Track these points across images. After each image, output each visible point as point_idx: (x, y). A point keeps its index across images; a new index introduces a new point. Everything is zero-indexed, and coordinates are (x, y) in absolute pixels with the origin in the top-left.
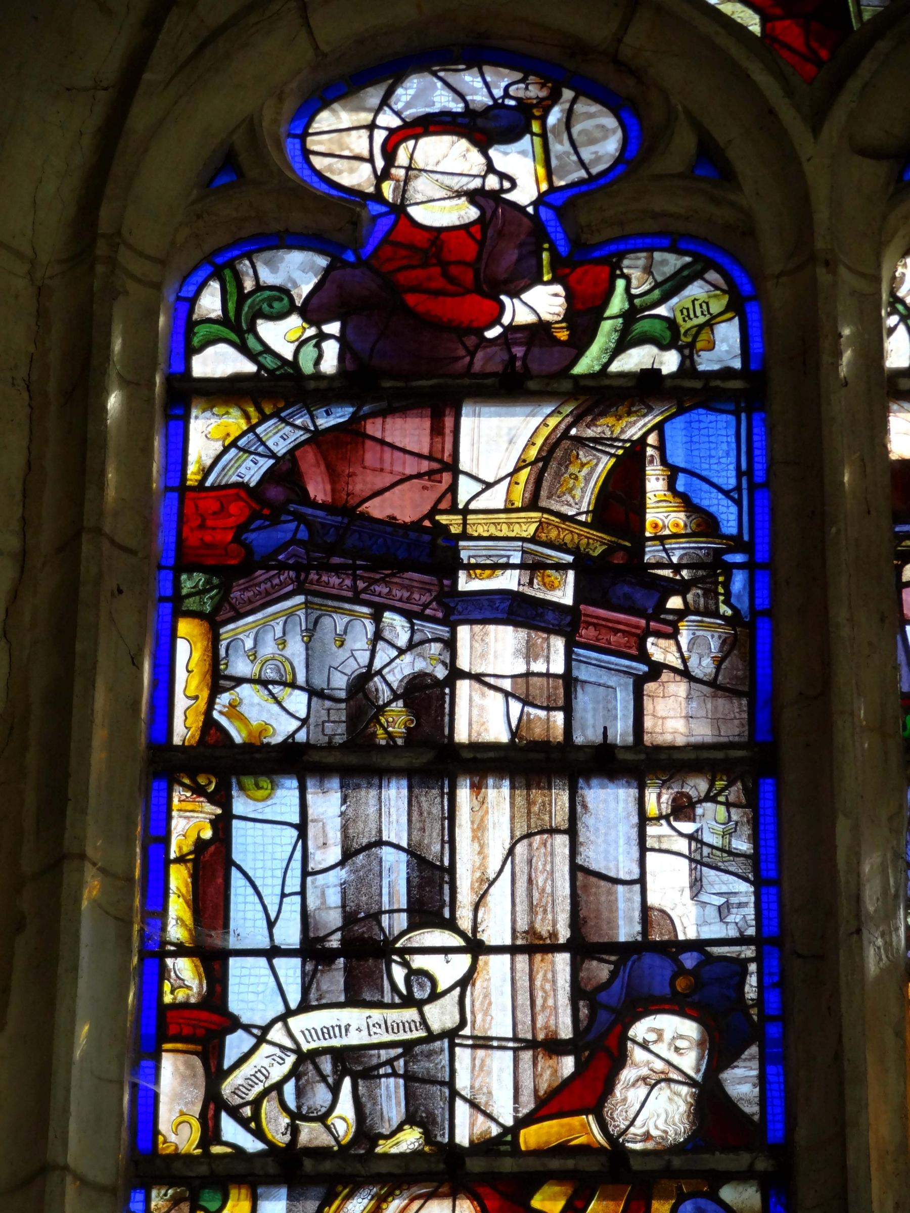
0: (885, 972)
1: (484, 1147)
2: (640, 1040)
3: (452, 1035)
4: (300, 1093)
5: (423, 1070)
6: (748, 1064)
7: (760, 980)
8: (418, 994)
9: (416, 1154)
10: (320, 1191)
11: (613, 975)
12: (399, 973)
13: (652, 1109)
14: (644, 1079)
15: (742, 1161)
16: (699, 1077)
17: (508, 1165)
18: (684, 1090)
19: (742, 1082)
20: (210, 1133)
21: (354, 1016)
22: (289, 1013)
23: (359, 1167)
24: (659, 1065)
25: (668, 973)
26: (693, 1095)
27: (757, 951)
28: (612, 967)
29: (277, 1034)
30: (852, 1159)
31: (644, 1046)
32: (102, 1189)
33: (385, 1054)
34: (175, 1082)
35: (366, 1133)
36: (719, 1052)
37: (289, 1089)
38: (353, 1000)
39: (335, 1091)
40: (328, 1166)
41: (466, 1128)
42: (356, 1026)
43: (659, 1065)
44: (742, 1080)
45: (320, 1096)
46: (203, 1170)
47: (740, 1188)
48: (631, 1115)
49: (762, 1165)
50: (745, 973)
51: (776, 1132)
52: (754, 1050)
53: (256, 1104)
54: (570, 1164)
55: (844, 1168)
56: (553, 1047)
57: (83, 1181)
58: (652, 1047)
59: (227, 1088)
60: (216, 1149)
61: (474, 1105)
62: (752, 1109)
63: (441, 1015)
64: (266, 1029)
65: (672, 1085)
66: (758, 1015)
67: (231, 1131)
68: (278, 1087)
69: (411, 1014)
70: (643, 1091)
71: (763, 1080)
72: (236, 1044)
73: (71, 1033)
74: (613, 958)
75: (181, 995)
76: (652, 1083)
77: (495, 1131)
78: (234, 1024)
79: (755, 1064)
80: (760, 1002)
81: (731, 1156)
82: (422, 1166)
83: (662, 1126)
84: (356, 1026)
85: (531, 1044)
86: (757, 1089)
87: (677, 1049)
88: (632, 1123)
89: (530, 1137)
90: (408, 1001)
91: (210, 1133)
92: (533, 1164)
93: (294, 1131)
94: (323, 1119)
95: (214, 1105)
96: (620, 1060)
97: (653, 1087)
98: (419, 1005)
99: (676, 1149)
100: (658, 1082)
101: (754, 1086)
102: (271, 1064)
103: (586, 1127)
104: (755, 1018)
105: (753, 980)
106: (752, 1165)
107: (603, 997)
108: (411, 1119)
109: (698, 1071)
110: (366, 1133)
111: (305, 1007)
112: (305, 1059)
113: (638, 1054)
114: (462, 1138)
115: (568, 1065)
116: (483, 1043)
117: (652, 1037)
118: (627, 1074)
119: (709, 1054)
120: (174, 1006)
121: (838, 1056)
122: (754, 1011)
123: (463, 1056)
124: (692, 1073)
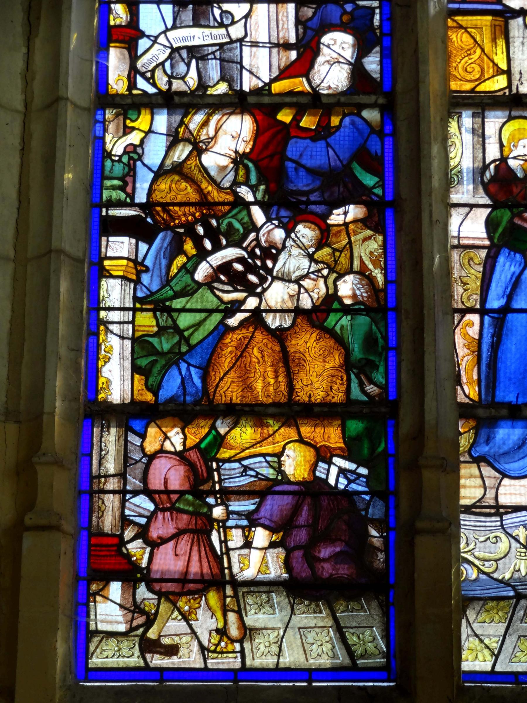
0: (438, 13)
1: (256, 92)
2: (326, 44)
3: (241, 41)
4: (172, 66)
5: (228, 56)
6: (375, 55)
7: (381, 17)
8: (226, 22)
9: (225, 95)
10: (182, 111)
11: (314, 14)
12: (217, 12)
13: (331, 74)
14: (328, 61)
15: (372, 99)
16: (353, 61)
17: (266, 100)
18: (346, 67)
19: (372, 64)
20: (132, 85)
21: (197, 32)
22: (167, 30)
23: (199, 101)
24: (335, 56)
25: (339, 14)
26: (350, 69)
27: (380, 3)
28: (314, 10)
29: (162, 39)
30: (421, 98)
31: (328, 46)
32: (84, 109)
33: (211, 49)
34: (116, 61)
35: (202, 85)
36: (362, 49)
37: (168, 65)
38: (196, 24)
39: (188, 65)
40: (185, 100)
41: (248, 83)
42: (198, 36)
43: (335, 56)
44: (372, 63)
45: (182, 68)
46: (129, 101)
47: (371, 111)
48: (322, 78)
49: (381, 101)
50: (374, 13)
51: (387, 87)
52: (378, 49)
53: (153, 71)
54: (295, 100)
55: (418, 101)
56: (287, 46)
57: (75, 106)
58: (331, 47)
59: (139, 64)
60: (135, 92)
61: (251, 73)
62: (376, 76)
63: (236, 32)
64: (157, 37)
65: (341, 64)
66: (380, 33)
67: (142, 84)
68: (162, 64)
69: (223, 31)
70: (327, 66)
71: (381, 62)
72: (143, 44)
73: (69, 38)
74: (314, 6)
75: (118, 21)
76: (332, 63)
77: (261, 84)
78: (142, 35)
79: (378, 55)
80: (381, 27)
81: (367, 97)
82: (227, 100)
83: (337, 84)
84: (198, 36)
85: (277, 45)
86: (379, 67)
87: (343, 48)
88: (322, 82)
89: (277, 88)
90: (221, 25)
91: (132, 85)
92: (277, 100)
93: (170, 83)
94: (183, 78)
95: (134, 72)
96: (317, 52)
97: (332, 65)
98: (226, 27)
99: (343, 93)
100: (334, 63)
101: (378, 65)
102: (158, 53)
103: (302, 83)
104: (378, 34)
105: (377, 17)
106: (376, 101)
107: (309, 24)
108: (223, 79)
109: (352, 58)
110: (202, 85)
111: (174, 27)
112: (175, 51)
113: (324, 50)
114: (246, 88)
115: (293, 55)
116: (255, 44)
117: (331, 42)
118: (320, 60)
119: (358, 51)
120: (115, 26)
121: (416, 51)
122: (378, 31)
123: (246, 50)
124: (350, 59)
